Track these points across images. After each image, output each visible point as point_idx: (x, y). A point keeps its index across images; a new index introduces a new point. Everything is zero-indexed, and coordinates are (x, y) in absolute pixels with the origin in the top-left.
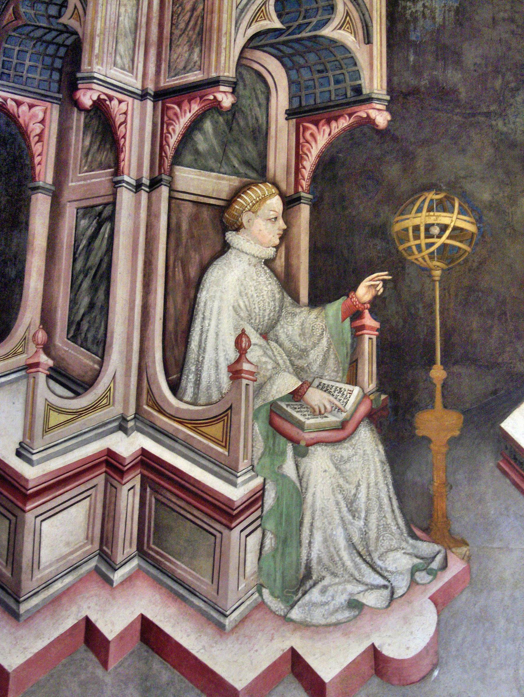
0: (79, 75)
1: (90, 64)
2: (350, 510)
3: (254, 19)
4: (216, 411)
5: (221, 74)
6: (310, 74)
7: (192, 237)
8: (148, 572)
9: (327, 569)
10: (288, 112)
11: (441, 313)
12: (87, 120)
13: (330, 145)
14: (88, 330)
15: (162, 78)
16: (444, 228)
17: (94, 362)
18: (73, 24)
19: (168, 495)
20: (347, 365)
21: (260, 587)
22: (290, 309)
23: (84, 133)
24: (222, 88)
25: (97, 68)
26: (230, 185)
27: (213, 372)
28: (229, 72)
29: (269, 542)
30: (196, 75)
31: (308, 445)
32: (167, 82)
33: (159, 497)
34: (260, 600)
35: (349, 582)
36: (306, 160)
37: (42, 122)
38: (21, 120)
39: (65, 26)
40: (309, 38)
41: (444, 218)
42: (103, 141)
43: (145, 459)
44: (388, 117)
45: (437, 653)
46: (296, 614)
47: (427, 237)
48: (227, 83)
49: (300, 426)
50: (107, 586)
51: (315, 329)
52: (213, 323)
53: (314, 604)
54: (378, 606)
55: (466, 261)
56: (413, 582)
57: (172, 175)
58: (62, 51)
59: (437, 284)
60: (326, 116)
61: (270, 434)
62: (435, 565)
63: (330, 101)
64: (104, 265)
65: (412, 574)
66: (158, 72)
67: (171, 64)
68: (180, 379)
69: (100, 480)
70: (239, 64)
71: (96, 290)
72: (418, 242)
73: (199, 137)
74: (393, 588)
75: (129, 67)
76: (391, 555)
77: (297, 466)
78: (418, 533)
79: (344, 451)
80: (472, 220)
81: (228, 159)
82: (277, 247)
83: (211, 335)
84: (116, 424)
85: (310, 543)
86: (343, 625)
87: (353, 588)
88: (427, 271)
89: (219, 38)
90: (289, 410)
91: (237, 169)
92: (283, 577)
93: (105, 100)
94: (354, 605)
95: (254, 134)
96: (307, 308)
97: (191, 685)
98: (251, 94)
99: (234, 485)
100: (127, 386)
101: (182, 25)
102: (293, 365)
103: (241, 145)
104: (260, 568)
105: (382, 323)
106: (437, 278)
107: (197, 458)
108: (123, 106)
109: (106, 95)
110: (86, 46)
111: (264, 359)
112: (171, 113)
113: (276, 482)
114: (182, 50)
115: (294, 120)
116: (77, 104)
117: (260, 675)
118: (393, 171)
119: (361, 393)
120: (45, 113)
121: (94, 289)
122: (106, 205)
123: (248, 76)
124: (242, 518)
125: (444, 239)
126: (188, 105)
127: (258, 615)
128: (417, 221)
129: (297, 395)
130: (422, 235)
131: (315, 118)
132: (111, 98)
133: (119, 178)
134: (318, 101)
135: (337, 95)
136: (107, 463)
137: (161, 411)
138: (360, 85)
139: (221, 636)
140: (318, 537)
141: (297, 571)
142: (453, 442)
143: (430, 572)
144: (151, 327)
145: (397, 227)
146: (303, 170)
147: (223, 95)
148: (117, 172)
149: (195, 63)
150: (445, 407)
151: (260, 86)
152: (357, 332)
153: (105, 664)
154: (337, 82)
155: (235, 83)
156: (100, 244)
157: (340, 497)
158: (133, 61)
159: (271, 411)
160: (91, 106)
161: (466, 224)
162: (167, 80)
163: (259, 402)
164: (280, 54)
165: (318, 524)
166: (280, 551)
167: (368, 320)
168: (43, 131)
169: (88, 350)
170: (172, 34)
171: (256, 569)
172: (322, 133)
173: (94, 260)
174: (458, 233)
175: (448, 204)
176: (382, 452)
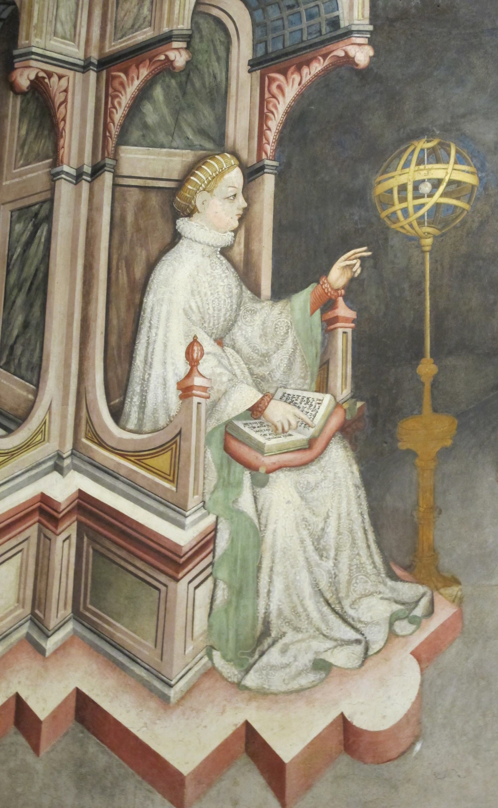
0: (16, 52)
1: (28, 37)
2: (316, 549)
4: (163, 438)
5: (175, 27)
6: (278, 10)
7: (138, 230)
8: (83, 638)
9: (289, 623)
10: (251, 63)
11: (432, 291)
12: (24, 105)
13: (300, 97)
14: (22, 354)
15: (107, 42)
16: (436, 184)
17: (28, 391)
19: (108, 544)
20: (316, 369)
21: (210, 650)
22: (250, 305)
23: (20, 121)
24: (175, 45)
26: (183, 161)
27: (160, 391)
28: (183, 23)
29: (222, 594)
30: (145, 33)
31: (269, 472)
32: (113, 46)
33: (98, 547)
34: (210, 665)
35: (314, 637)
36: (271, 119)
41: (438, 171)
43: (83, 503)
44: (369, 51)
45: (419, 722)
46: (252, 680)
47: (415, 198)
48: (181, 37)
49: (259, 448)
50: (39, 657)
51: (279, 328)
52: (161, 333)
53: (273, 668)
54: (349, 665)
55: (464, 222)
56: (392, 634)
57: (117, 158)
59: (428, 256)
60: (296, 61)
61: (225, 462)
62: (418, 612)
63: (302, 41)
64: (40, 275)
65: (391, 625)
66: (103, 36)
67: (118, 24)
68: (123, 403)
69: (33, 532)
70: (195, 12)
71: (31, 306)
72: (404, 205)
73: (148, 108)
74: (367, 643)
75: (71, 35)
76: (365, 602)
77: (255, 499)
78: (399, 572)
79: (311, 475)
80: (472, 169)
81: (180, 128)
82: (235, 231)
83: (159, 347)
84: (51, 463)
85: (269, 592)
86: (307, 693)
87: (320, 645)
88: (415, 241)
90: (246, 430)
91: (191, 140)
92: (237, 635)
93: (44, 78)
94: (321, 666)
95: (212, 95)
96: (270, 303)
97: (131, 771)
98: (208, 46)
99: (182, 526)
100: (64, 417)
102: (252, 374)
103: (195, 112)
104: (210, 626)
105: (359, 312)
106: (427, 248)
107: (141, 497)
108: (64, 81)
110: (24, 17)
111: (219, 370)
112: (116, 83)
113: (230, 519)
115: (258, 72)
116: (12, 86)
117: (208, 758)
118: (375, 121)
119: (333, 403)
121: (29, 305)
122: (44, 202)
123: (205, 26)
124: (190, 566)
125: (437, 198)
126: (136, 71)
127: (207, 683)
128: (402, 179)
129: (256, 411)
130: (410, 195)
131: (283, 65)
132: (50, 75)
133: (58, 169)
134: (288, 43)
135: (309, 34)
136: (41, 511)
137: (101, 444)
138: (338, 17)
139: (165, 710)
140: (278, 585)
141: (254, 627)
142: (445, 453)
143: (415, 621)
144: (91, 344)
145: (380, 189)
146: (268, 132)
147: (176, 53)
148: (56, 162)
149: (145, 18)
150: (435, 410)
151: (219, 36)
152: (329, 325)
153: (36, 749)
154: (310, 17)
155: (190, 36)
156: (36, 250)
157: (305, 533)
158: (75, 27)
159: (227, 433)
160: (28, 88)
161: (466, 176)
162: (113, 44)
163: (213, 423)
165: (278, 568)
166: (234, 604)
167: (343, 310)
169: (22, 378)
171: (205, 628)
172: (291, 84)
173: (29, 270)
174: (455, 188)
175: (442, 153)
176: (357, 474)
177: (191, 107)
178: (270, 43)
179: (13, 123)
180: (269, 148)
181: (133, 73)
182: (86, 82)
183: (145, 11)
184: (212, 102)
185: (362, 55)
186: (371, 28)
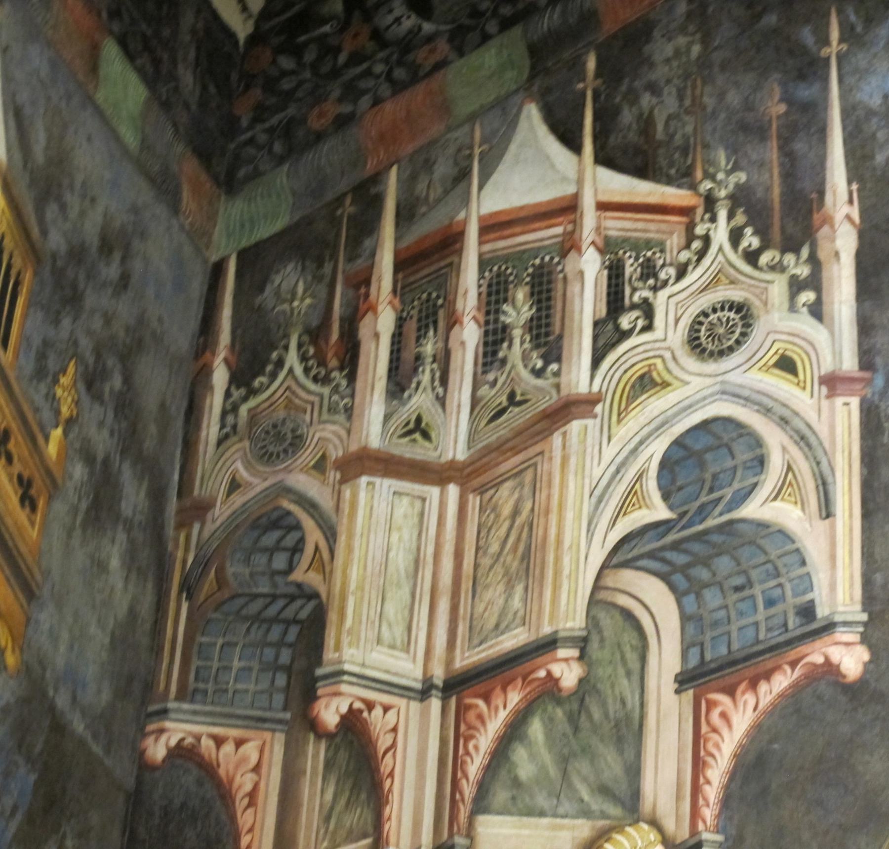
1: (338, 647)
3: (621, 511)
5: (561, 626)
6: (719, 593)
10: (680, 678)
12: (330, 754)
13: (757, 730)
15: (458, 652)
18: (313, 579)
23: (324, 779)
25: (348, 652)
26: (573, 839)
28: (573, 620)
30: (515, 636)
36: (712, 767)
37: (257, 769)
38: (222, 772)
39: (299, 586)
40: (720, 529)
42: (355, 788)
44: (863, 654)
48: (571, 641)
57: (472, 834)
58: (293, 633)
60: (750, 672)
63: (758, 642)
67: (475, 623)
70: (593, 602)
73: (520, 754)
75: (402, 641)
81: (570, 786)
89: (558, 559)
91: (588, 805)
93: (361, 711)
95: (618, 731)
98: (613, 654)
101: (494, 548)
103: (593, 758)
108: (391, 715)
109: (364, 701)
110: (332, 617)
112: (471, 716)
114: (494, 594)
115: (691, 692)
116: (313, 725)
120: (261, 752)
123: (608, 622)
126: (503, 696)
131: (729, 680)
132: (370, 706)
134: (735, 646)
135: (769, 630)
138: (812, 602)
146: (707, 788)
147: (563, 665)
149: (515, 613)
151: (629, 638)
154: (770, 603)
158: (409, 629)
160: (337, 726)
162: (467, 654)
164: (665, 568)
168: (256, 786)
170: (476, 566)
172: (741, 708)
177: (587, 751)
178: (708, 646)
179: (313, 784)
180: (709, 813)
181: (498, 700)
182: (425, 716)
183: (516, 602)
184: (619, 742)
185: (851, 659)
186: (864, 617)
